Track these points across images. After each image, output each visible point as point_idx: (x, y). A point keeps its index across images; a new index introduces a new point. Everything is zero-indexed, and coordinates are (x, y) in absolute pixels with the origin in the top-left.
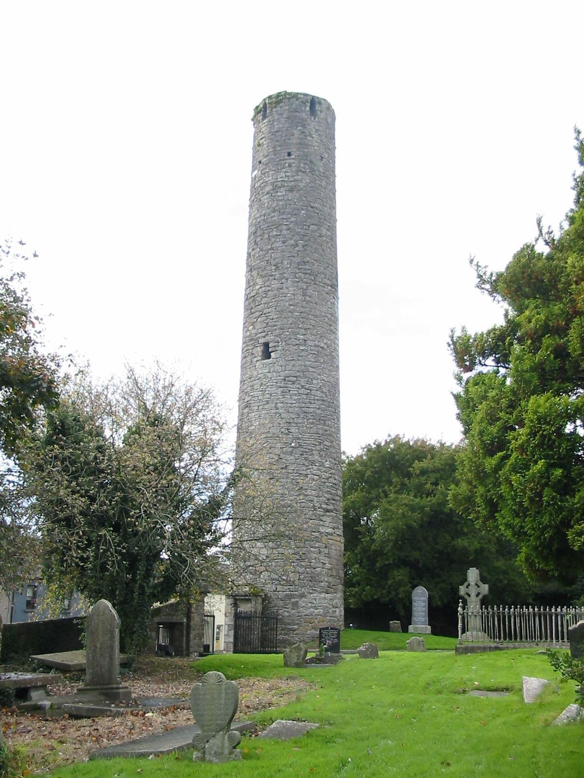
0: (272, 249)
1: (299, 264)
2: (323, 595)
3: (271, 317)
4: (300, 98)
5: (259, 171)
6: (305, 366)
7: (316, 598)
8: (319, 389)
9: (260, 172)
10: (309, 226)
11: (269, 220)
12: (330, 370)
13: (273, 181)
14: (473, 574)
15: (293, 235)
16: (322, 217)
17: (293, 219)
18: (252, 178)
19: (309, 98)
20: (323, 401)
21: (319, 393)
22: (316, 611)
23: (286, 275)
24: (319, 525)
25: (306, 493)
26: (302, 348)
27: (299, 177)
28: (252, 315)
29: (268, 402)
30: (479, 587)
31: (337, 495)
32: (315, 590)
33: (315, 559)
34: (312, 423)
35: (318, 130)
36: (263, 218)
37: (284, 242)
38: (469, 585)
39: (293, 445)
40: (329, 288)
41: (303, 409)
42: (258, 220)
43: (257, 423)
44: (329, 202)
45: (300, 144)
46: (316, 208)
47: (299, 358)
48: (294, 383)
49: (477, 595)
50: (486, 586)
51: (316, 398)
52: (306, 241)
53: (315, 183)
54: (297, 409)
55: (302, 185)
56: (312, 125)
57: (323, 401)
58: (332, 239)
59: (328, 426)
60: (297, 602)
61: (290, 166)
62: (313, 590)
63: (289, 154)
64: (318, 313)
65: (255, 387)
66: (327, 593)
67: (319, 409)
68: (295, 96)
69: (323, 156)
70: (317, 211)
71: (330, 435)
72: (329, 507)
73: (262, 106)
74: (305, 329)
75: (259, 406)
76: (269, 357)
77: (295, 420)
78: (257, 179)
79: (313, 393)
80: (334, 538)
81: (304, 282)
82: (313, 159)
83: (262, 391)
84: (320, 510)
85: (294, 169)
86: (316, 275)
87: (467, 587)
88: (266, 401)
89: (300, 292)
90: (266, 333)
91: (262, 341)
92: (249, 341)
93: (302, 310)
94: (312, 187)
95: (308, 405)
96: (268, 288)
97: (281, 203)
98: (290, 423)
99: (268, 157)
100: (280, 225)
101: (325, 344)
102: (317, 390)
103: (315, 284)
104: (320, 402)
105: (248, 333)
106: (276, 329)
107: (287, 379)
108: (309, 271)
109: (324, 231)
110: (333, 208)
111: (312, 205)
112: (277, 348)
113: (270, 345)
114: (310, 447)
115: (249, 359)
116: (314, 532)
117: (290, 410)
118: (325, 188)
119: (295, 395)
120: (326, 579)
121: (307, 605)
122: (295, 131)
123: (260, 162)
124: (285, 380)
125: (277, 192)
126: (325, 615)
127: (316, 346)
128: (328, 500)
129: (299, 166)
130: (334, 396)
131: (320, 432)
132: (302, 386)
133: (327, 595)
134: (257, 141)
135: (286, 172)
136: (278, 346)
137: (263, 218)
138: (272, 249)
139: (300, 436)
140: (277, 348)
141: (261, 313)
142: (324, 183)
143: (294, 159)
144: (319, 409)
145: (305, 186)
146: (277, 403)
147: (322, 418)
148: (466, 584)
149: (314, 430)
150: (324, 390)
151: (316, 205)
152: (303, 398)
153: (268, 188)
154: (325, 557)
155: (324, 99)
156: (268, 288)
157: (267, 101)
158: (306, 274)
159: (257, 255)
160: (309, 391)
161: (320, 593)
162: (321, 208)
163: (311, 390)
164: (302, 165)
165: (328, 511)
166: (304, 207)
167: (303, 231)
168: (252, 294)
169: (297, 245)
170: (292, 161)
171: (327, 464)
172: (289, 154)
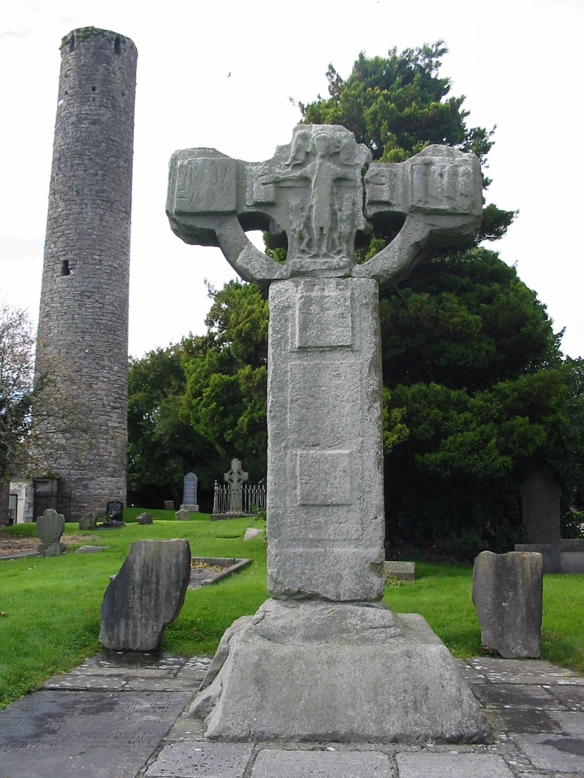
0: (74, 176)
1: (98, 192)
2: (109, 479)
3: (71, 238)
4: (106, 36)
5: (65, 101)
6: (100, 283)
8: (111, 304)
9: (66, 102)
10: (108, 158)
11: (73, 149)
12: (121, 288)
13: (77, 112)
14: (236, 464)
15: (94, 165)
16: (120, 150)
17: (94, 150)
18: (58, 106)
19: (115, 36)
20: (114, 314)
21: (111, 308)
22: (103, 492)
23: (85, 201)
25: (97, 393)
26: (97, 267)
27: (102, 112)
28: (53, 235)
29: (66, 313)
30: (240, 474)
31: (123, 395)
33: (103, 448)
35: (121, 68)
36: (67, 146)
37: (85, 171)
38: (232, 472)
39: (87, 351)
40: (124, 214)
41: (96, 321)
42: (63, 147)
43: (56, 331)
44: (128, 136)
45: (103, 80)
46: (115, 141)
47: (95, 276)
48: (89, 297)
49: (239, 481)
50: (246, 474)
51: (108, 311)
52: (105, 171)
53: (116, 118)
54: (91, 321)
55: (104, 119)
56: (116, 62)
57: (114, 314)
58: (128, 170)
59: (118, 336)
60: (87, 484)
61: (94, 100)
63: (94, 89)
64: (113, 237)
67: (110, 321)
68: (102, 33)
69: (124, 93)
70: (116, 144)
71: (119, 344)
72: (116, 405)
73: (70, 38)
74: (101, 251)
75: (57, 316)
76: (68, 273)
77: (90, 330)
78: (63, 109)
79: (105, 306)
80: (119, 431)
81: (101, 209)
82: (116, 96)
83: (60, 303)
85: (98, 103)
86: (113, 203)
87: (231, 474)
89: (98, 217)
91: (62, 259)
92: (50, 258)
93: (99, 233)
94: (113, 122)
95: (101, 317)
96: (69, 212)
97: (84, 134)
98: (84, 332)
99: (75, 89)
100: (83, 154)
101: (118, 264)
103: (111, 211)
104: (112, 315)
105: (50, 251)
106: (74, 250)
107: (83, 294)
108: (106, 199)
109: (122, 163)
110: (131, 141)
111: (112, 138)
112: (75, 266)
113: (70, 263)
115: (50, 274)
117: (85, 320)
118: (125, 123)
119: (90, 308)
122: (100, 68)
124: (81, 294)
125: (81, 124)
126: (110, 495)
127: (110, 266)
128: (116, 399)
129: (101, 101)
130: (123, 310)
131: (111, 341)
132: (96, 301)
133: (112, 479)
134: (64, 72)
135: (90, 106)
136: (77, 264)
137: (67, 146)
138: (74, 176)
139: (93, 344)
140: (75, 266)
141: (62, 234)
142: (123, 119)
143: (98, 94)
144: (110, 321)
145: (107, 121)
146: (74, 315)
148: (230, 472)
149: (106, 338)
150: (116, 305)
151: (116, 139)
152: (96, 311)
153: (73, 119)
155: (128, 38)
156: (69, 212)
157: (75, 34)
158: (104, 201)
159: (60, 180)
160: (102, 305)
161: (107, 476)
162: (120, 142)
164: (105, 101)
165: (115, 408)
166: (105, 140)
167: (102, 162)
168: (55, 216)
169: (97, 175)
170: (96, 96)
171: (116, 368)
172: (94, 89)
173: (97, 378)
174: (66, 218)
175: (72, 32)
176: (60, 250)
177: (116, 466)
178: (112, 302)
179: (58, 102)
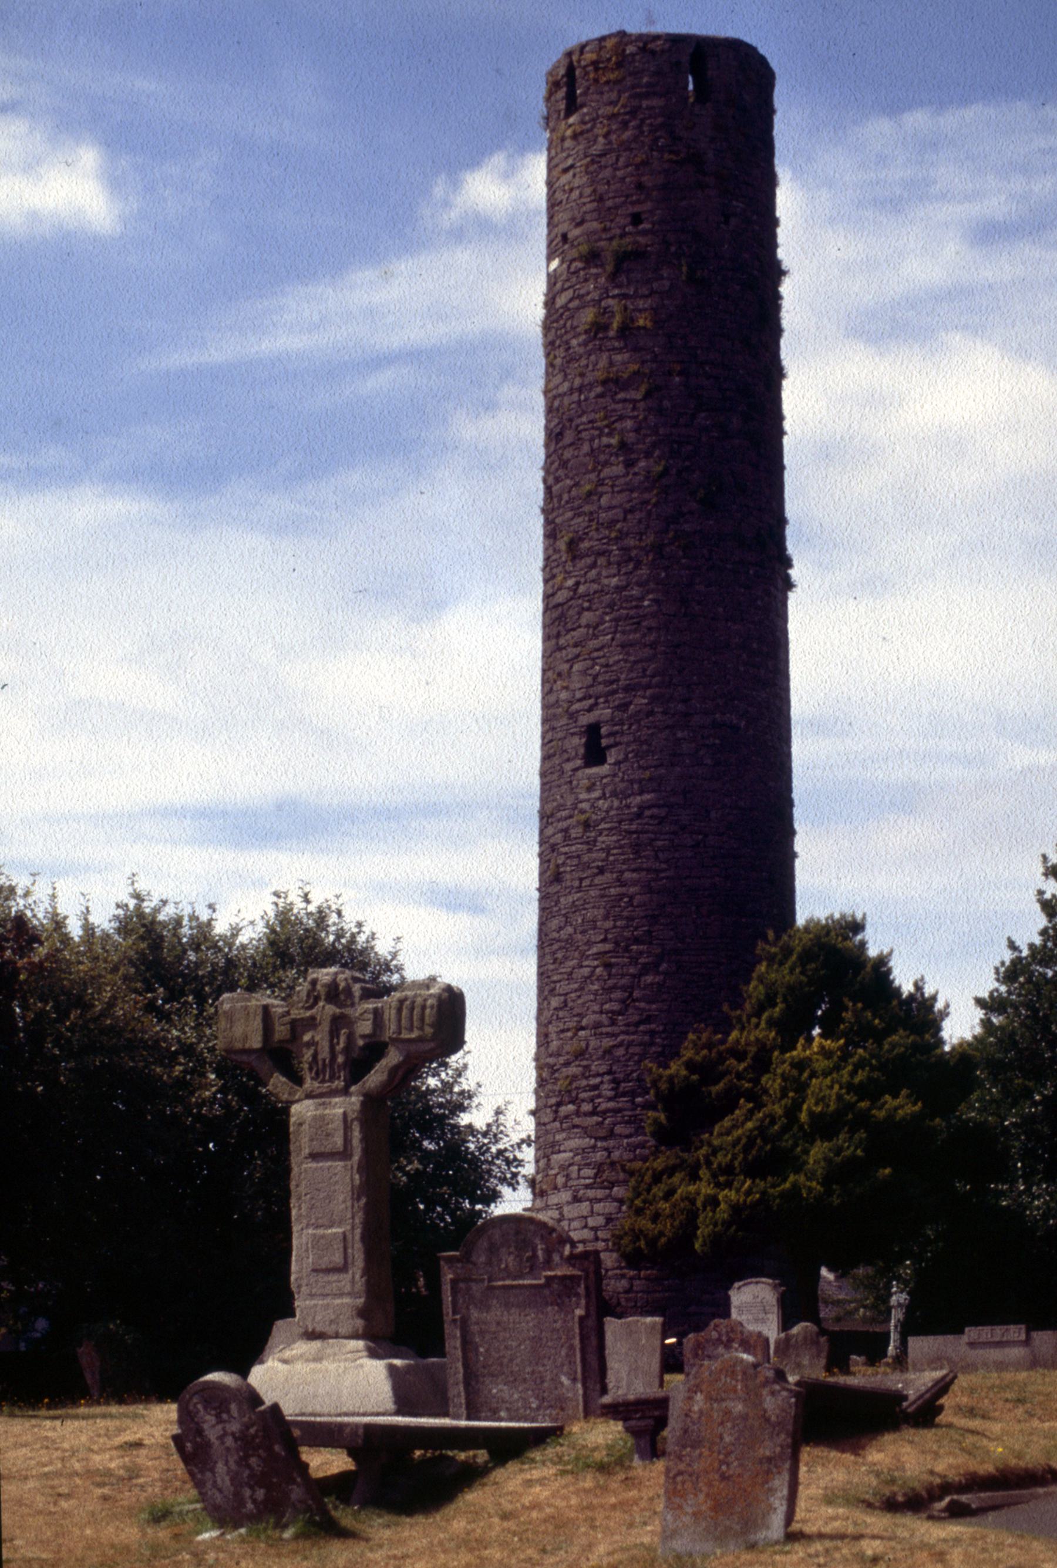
5: (562, 262)
9: (565, 266)
18: (548, 275)
28: (558, 655)
29: (601, 871)
36: (575, 397)
65: (574, 833)
73: (562, 71)
75: (581, 880)
78: (559, 285)
83: (588, 843)
88: (598, 867)
90: (592, 701)
91: (585, 720)
99: (585, 226)
106: (614, 692)
113: (604, 731)
115: (556, 760)
123: (565, 237)
146: (622, 872)
159: (566, 497)
174: (586, 605)
175: (569, 54)
176: (579, 695)
179: (548, 266)
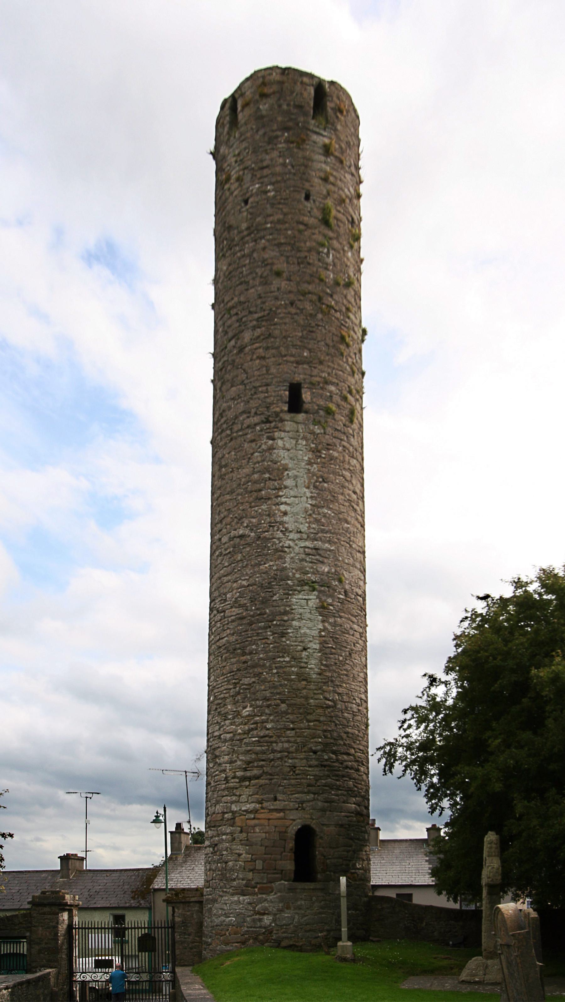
2: (236, 898)
7: (227, 902)
21: (235, 611)
24: (232, 803)
32: (226, 892)
34: (226, 659)
59: (251, 653)
62: (223, 891)
66: (244, 895)
71: (253, 667)
72: (248, 774)
84: (232, 780)
102: (232, 607)
114: (222, 696)
116: (227, 813)
120: (241, 876)
121: (218, 911)
126: (239, 925)
127: (231, 539)
128: (248, 763)
147: (238, 646)
150: (243, 601)
154: (242, 845)
161: (233, 895)
163: (224, 611)
165: (250, 779)
171: (245, 712)
173: (219, 737)
177: (250, 875)
178: (236, 602)
